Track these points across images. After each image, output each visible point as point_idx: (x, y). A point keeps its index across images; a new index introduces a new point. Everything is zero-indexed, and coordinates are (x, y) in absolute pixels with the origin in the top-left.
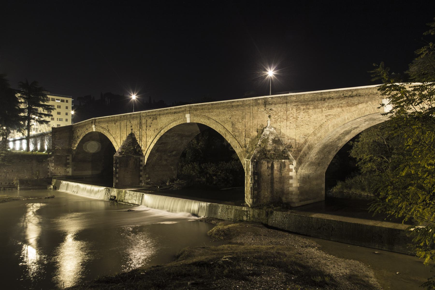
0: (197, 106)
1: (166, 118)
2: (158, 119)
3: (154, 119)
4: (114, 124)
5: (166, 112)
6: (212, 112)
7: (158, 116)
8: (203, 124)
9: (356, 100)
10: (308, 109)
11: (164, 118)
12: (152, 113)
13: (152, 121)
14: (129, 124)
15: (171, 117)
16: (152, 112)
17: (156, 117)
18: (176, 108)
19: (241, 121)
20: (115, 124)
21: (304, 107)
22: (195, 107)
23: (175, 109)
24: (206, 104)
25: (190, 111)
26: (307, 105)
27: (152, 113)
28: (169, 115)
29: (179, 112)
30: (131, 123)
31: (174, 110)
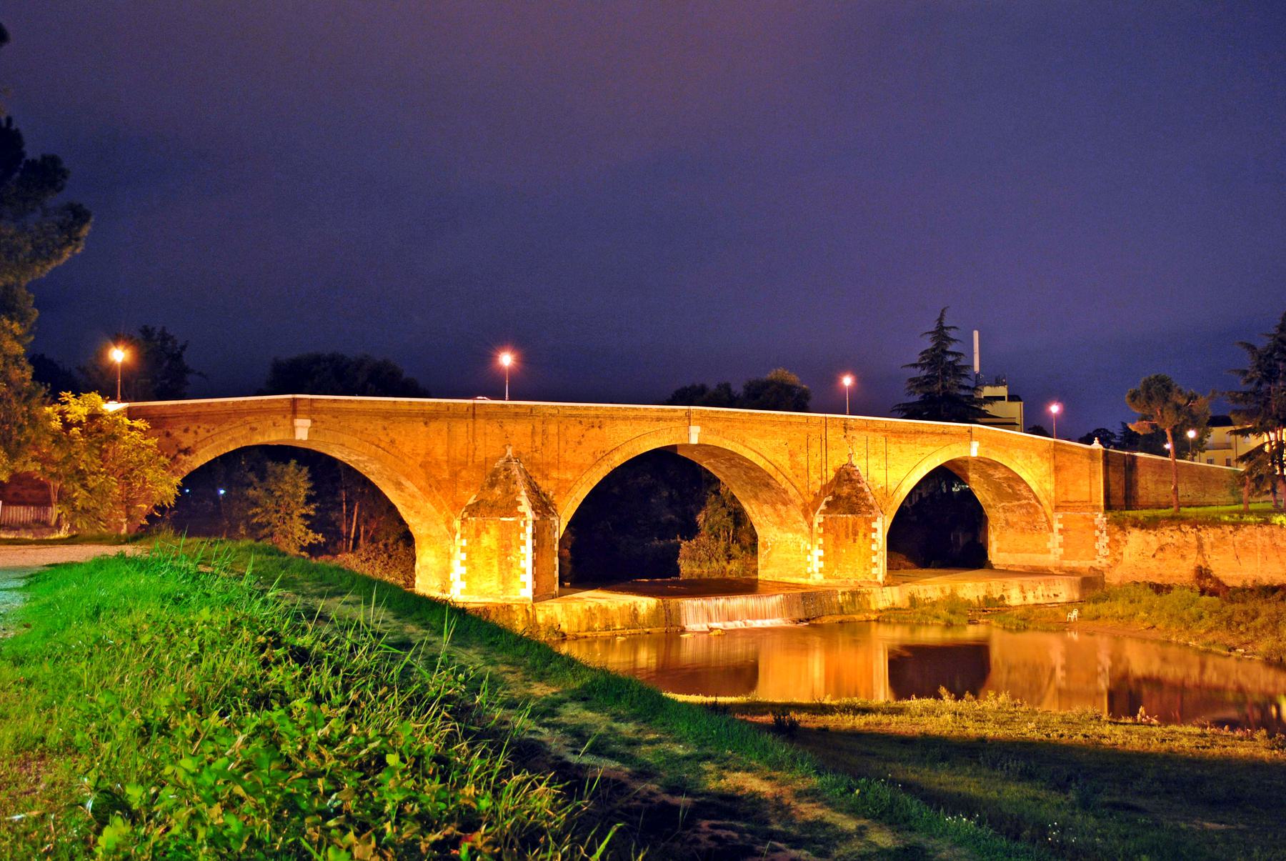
0: (718, 412)
1: (631, 428)
2: (607, 429)
3: (593, 427)
4: (422, 424)
5: (632, 414)
6: (751, 429)
7: (608, 421)
8: (729, 448)
9: (947, 438)
10: (900, 443)
11: (624, 428)
12: (586, 412)
13: (587, 430)
14: (497, 431)
15: (646, 427)
16: (586, 409)
17: (600, 422)
18: (663, 410)
19: (806, 451)
20: (426, 423)
21: (895, 439)
22: (711, 415)
23: (658, 410)
24: (737, 413)
25: (702, 420)
26: (899, 437)
27: (586, 412)
28: (643, 422)
29: (671, 420)
30: (505, 428)
31: (656, 414)
